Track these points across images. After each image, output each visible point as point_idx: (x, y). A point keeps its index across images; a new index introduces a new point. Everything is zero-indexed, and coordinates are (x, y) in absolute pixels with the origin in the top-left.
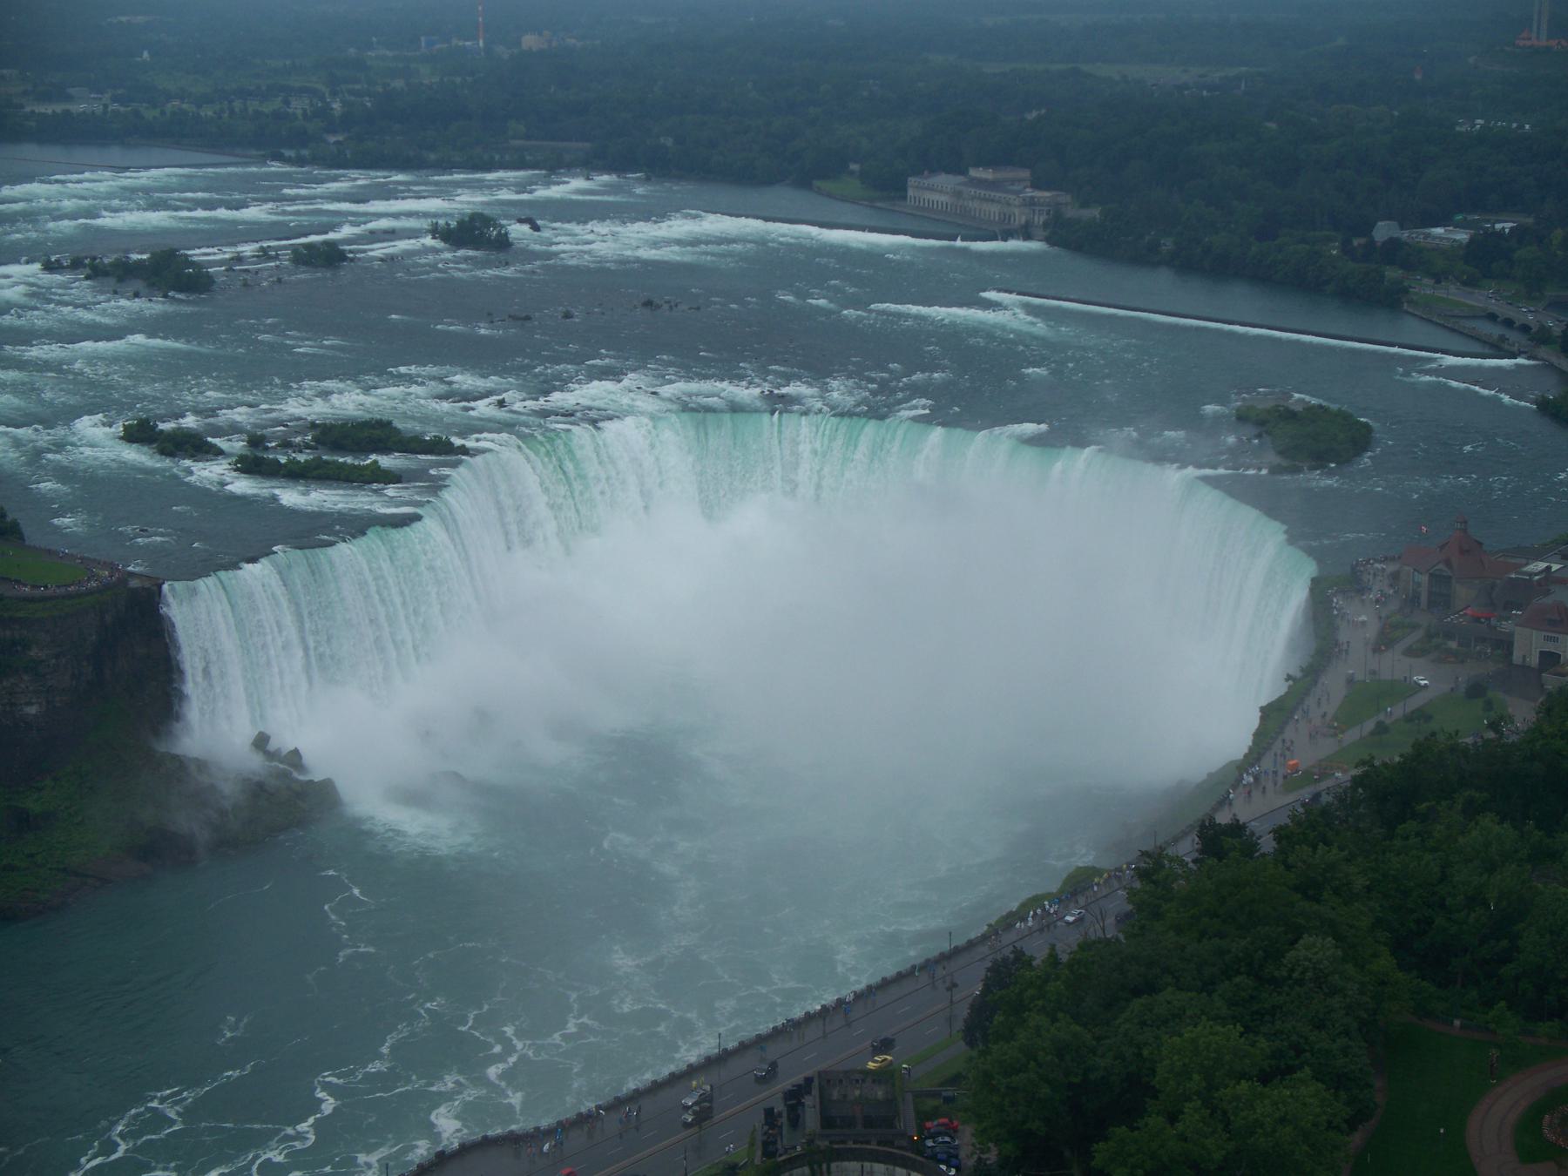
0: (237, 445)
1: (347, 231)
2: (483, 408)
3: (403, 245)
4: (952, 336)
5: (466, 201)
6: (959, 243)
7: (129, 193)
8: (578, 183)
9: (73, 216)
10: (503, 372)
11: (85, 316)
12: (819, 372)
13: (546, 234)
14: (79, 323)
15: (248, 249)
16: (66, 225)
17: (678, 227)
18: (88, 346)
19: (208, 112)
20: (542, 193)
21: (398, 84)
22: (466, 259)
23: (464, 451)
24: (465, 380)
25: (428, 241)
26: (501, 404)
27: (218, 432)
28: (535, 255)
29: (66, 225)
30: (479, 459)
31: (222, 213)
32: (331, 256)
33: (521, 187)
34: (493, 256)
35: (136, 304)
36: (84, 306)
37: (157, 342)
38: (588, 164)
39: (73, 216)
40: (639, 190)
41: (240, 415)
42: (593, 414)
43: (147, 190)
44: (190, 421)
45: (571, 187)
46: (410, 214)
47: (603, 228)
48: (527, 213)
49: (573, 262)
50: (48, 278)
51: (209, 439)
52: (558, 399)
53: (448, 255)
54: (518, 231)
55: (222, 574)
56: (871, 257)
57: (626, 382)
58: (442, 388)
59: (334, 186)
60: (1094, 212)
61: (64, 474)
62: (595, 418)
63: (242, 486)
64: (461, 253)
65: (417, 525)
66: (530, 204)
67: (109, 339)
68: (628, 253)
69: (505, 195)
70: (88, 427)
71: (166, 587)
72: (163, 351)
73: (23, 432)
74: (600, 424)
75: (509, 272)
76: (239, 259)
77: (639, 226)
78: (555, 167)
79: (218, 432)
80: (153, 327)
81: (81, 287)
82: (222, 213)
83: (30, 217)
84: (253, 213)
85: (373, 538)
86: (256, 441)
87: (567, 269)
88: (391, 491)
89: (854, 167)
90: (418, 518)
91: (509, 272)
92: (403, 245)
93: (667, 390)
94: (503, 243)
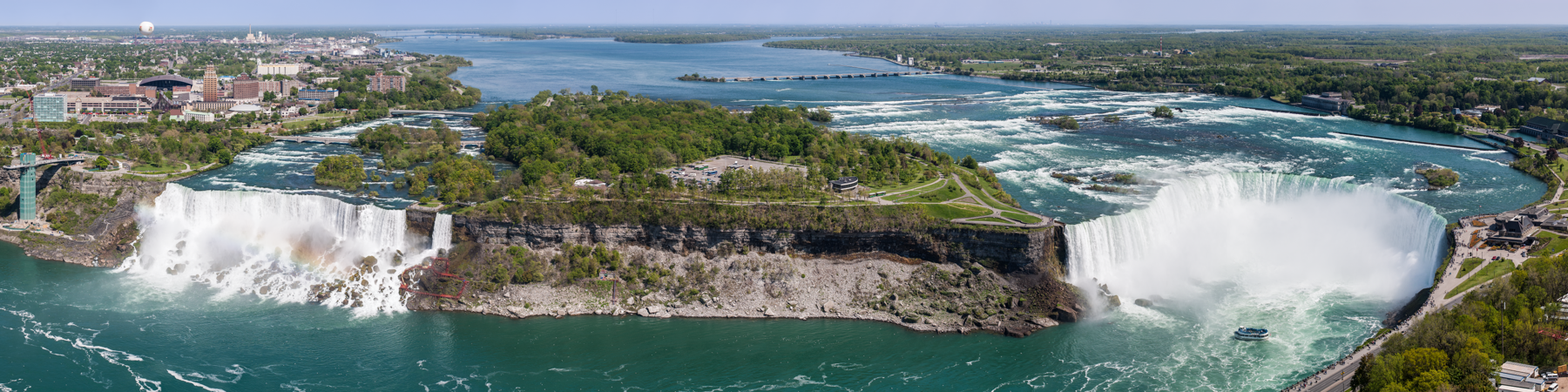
0: (1088, 179)
1: (1121, 111)
2: (1166, 170)
3: (1138, 116)
4: (1320, 148)
5: (1159, 102)
6: (1319, 117)
7: (1051, 97)
8: (1194, 97)
9: (1035, 104)
10: (1171, 158)
11: (1039, 136)
12: (1277, 159)
13: (1183, 113)
14: (1038, 139)
15: (1089, 116)
16: (1033, 107)
17: (1228, 111)
18: (1041, 146)
19: (1075, 73)
20: (1183, 100)
21: (1135, 65)
22: (1158, 121)
23: (1162, 184)
24: (1161, 161)
25: (1146, 115)
26: (1173, 168)
27: (1080, 175)
28: (1182, 120)
29: (1033, 107)
30: (1166, 188)
31: (1081, 104)
32: (1116, 120)
33: (1177, 98)
34: (1168, 119)
35: (1056, 133)
36: (1039, 133)
37: (1062, 145)
38: (1198, 90)
39: (1035, 104)
40: (1215, 99)
41: (1089, 170)
42: (1203, 173)
43: (1058, 97)
44: (1072, 171)
45: (1192, 98)
46: (1143, 106)
47: (1205, 111)
48: (1177, 106)
49: (1193, 122)
50: (1027, 124)
51: (1079, 178)
52: (1191, 168)
53: (1153, 120)
54: (1175, 112)
55: (1085, 223)
56: (1293, 122)
57: (1214, 162)
58: (1154, 163)
59: (1115, 97)
60: (1362, 107)
61: (1033, 186)
62: (1202, 174)
63: (1090, 193)
64: (1157, 119)
65: (1147, 209)
66: (1179, 103)
67: (1046, 143)
68: (1211, 120)
69: (1171, 100)
70: (1040, 171)
71: (1067, 226)
72: (1062, 148)
73: (1021, 172)
74: (1207, 178)
75: (1173, 125)
76: (1086, 120)
77: (1215, 111)
78: (1185, 92)
79: (1080, 175)
80: (1061, 140)
81: (1038, 128)
82: (1081, 104)
83: (1022, 104)
84: (1091, 105)
85: (1133, 212)
86: (1094, 180)
87: (1195, 126)
88: (1138, 197)
89: (1284, 93)
90: (1147, 206)
91: (1173, 125)
92: (1138, 116)
93: (1226, 165)
94: (1170, 117)
